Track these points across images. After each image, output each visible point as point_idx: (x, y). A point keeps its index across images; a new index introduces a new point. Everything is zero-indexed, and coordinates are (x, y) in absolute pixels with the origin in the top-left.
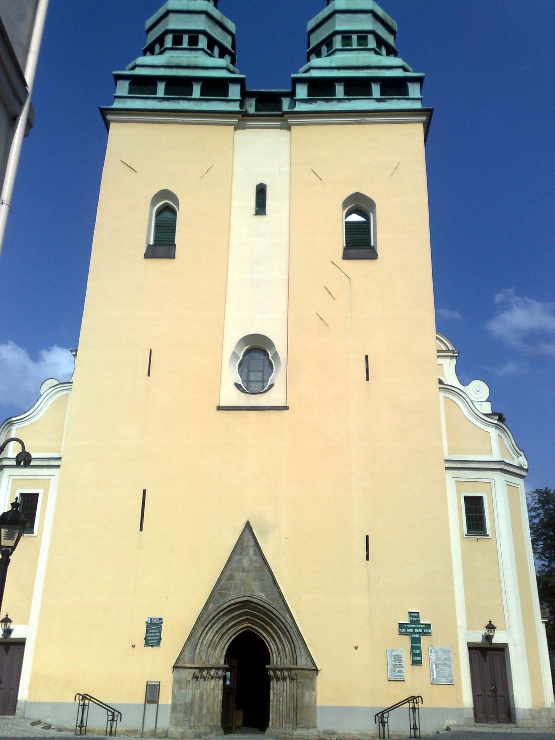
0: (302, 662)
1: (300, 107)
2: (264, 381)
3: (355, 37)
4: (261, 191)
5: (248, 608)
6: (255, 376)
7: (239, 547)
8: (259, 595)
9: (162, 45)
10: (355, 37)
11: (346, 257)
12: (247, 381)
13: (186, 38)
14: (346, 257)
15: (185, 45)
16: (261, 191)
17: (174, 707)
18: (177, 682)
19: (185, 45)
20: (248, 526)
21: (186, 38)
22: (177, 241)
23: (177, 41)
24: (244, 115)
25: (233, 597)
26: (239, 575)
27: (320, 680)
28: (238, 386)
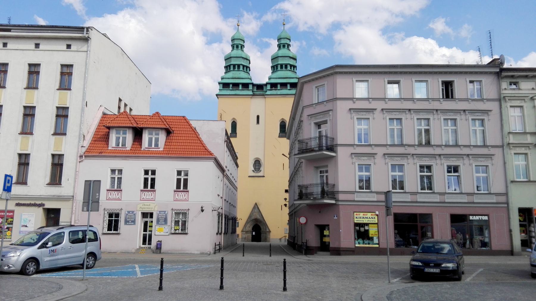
0: (268, 230)
1: (269, 93)
2: (259, 169)
3: (284, 66)
4: (258, 117)
5: (256, 220)
6: (257, 167)
7: (254, 208)
8: (258, 217)
9: (230, 69)
10: (284, 66)
11: (279, 137)
12: (255, 169)
13: (236, 66)
14: (279, 137)
15: (236, 69)
16: (258, 117)
17: (242, 238)
18: (242, 234)
19: (236, 69)
20: (256, 204)
21: (236, 66)
22: (237, 132)
23: (234, 67)
24: (254, 95)
25: (253, 218)
26: (254, 214)
27: (271, 234)
28: (253, 171)
